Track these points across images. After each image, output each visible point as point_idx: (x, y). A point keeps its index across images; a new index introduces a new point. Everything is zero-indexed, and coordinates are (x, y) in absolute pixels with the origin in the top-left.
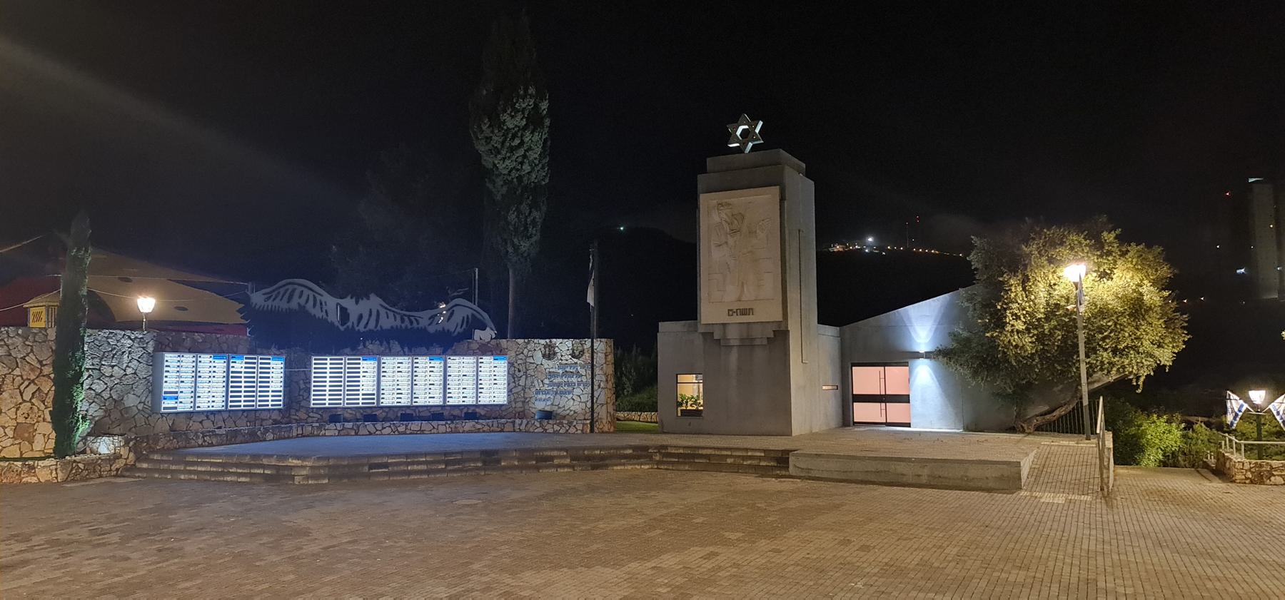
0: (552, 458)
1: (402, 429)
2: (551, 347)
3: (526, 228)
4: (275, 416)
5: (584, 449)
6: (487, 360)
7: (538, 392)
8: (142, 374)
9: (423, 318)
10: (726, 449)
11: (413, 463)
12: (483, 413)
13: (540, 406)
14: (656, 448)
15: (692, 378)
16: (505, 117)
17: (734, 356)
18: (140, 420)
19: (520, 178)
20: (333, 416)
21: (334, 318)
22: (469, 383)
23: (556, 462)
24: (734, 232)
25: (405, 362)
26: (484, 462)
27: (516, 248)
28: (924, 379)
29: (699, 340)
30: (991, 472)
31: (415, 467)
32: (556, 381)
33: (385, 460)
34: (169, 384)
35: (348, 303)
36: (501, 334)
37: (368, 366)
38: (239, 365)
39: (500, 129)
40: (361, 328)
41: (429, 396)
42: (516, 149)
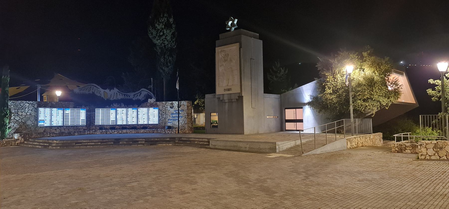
0: (138, 141)
1: (120, 132)
2: (172, 104)
3: (167, 64)
4: (84, 128)
5: (151, 138)
6: (151, 110)
7: (168, 120)
8: (33, 115)
9: (131, 95)
10: (197, 138)
11: (90, 142)
12: (151, 127)
13: (169, 124)
14: (178, 138)
15: (215, 114)
16: (157, 25)
17: (227, 106)
18: (33, 129)
19: (165, 46)
20: (101, 127)
21: (102, 96)
22: (146, 116)
23: (139, 142)
24: (225, 61)
25: (125, 110)
26: (114, 142)
27: (164, 71)
28: (308, 114)
29: (216, 100)
30: (267, 146)
31: (92, 144)
32: (174, 116)
33: (83, 141)
34: (41, 117)
35: (107, 91)
36: (157, 101)
37: (112, 112)
38: (68, 111)
39: (155, 29)
40: (112, 99)
41: (132, 121)
42: (163, 35)
